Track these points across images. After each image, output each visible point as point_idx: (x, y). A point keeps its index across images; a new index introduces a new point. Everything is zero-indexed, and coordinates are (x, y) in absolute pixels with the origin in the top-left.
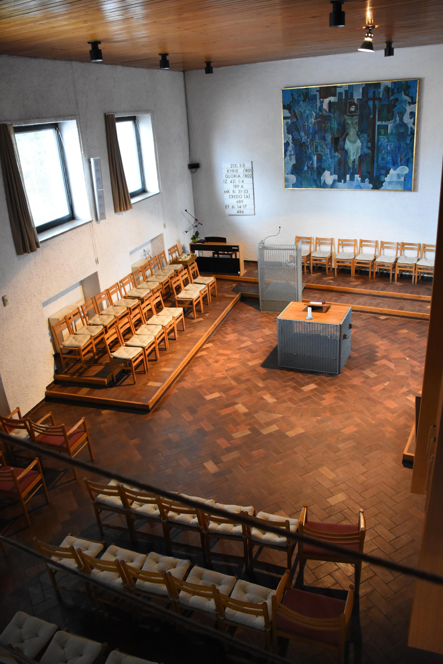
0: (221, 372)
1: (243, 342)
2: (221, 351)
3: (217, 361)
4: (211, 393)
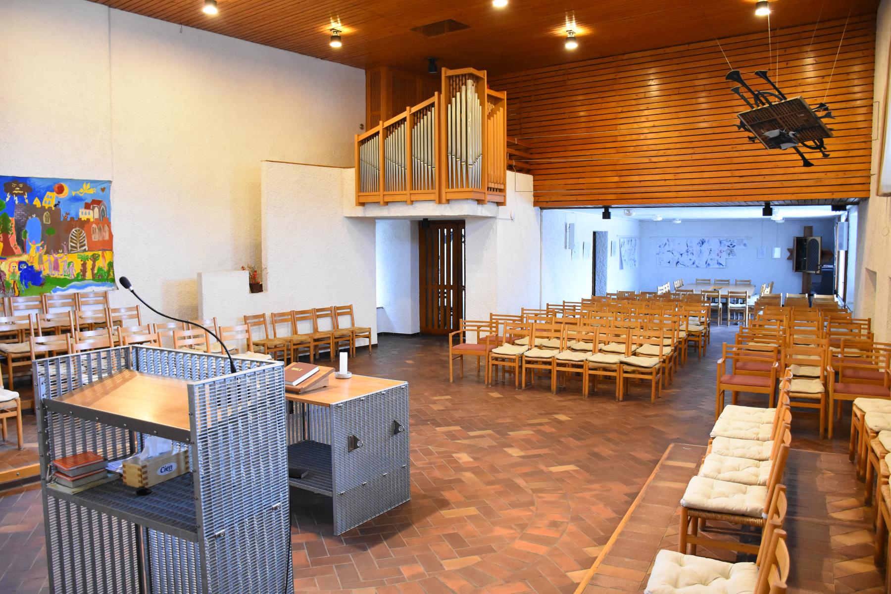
0: (546, 502)
1: (468, 572)
2: (542, 550)
3: (554, 524)
4: (567, 472)
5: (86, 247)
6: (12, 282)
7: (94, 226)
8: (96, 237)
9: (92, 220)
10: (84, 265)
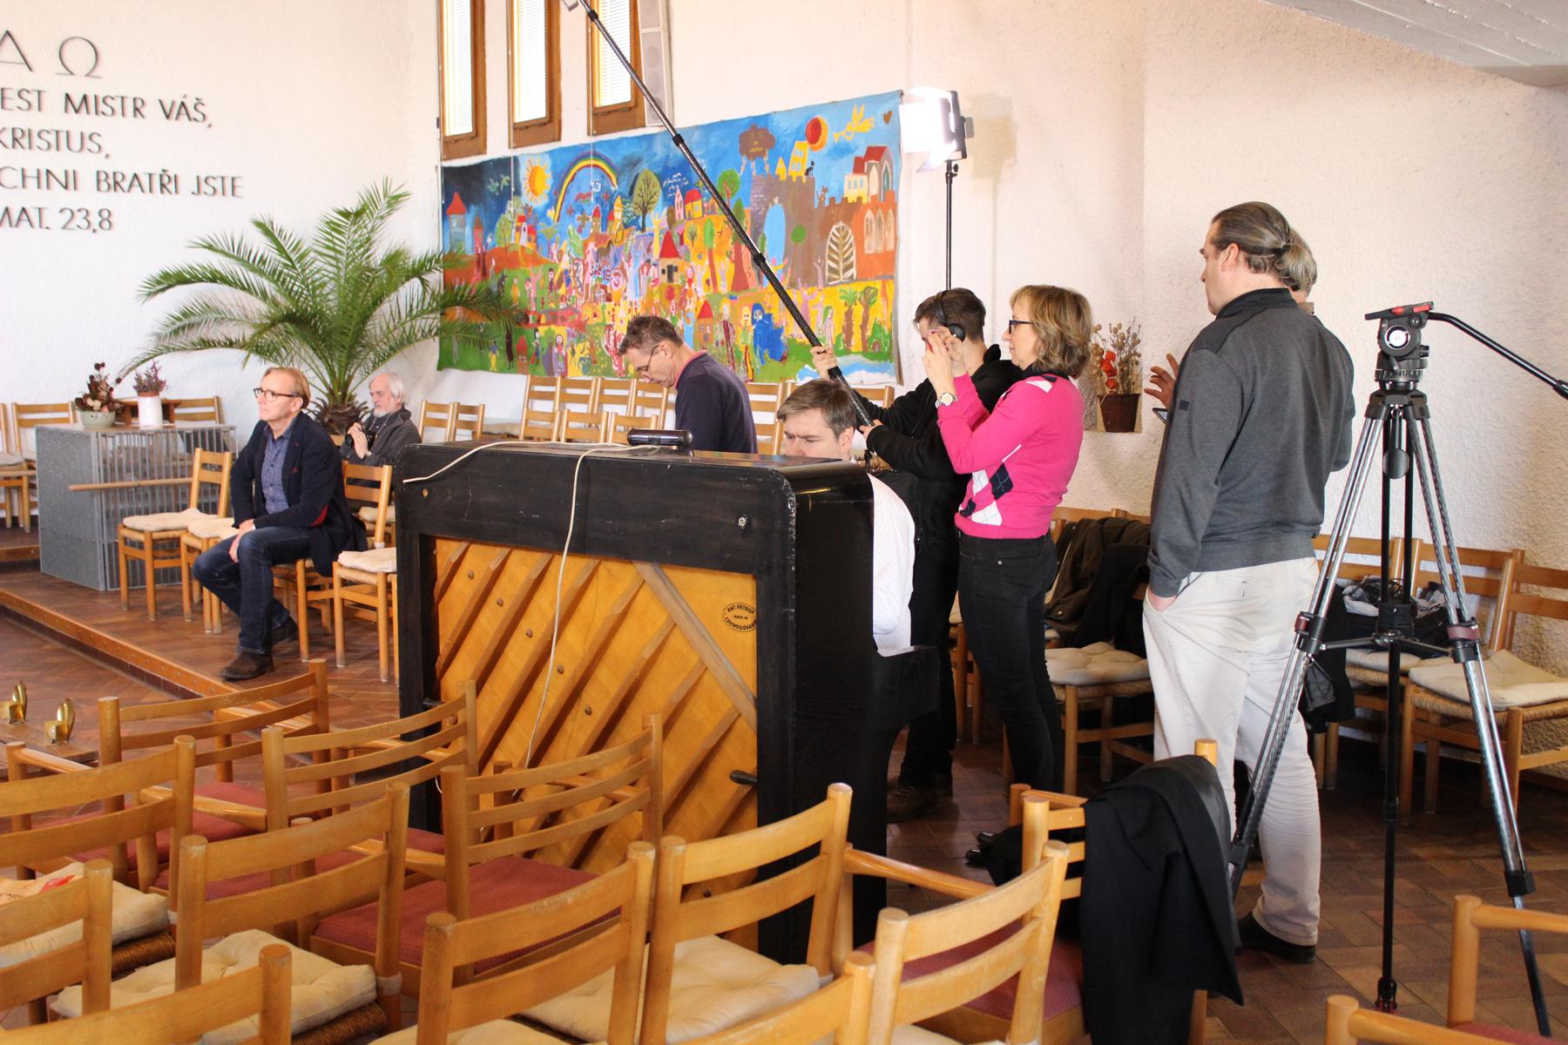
5: (853, 271)
6: (742, 349)
7: (869, 214)
8: (872, 246)
9: (865, 201)
10: (849, 315)
